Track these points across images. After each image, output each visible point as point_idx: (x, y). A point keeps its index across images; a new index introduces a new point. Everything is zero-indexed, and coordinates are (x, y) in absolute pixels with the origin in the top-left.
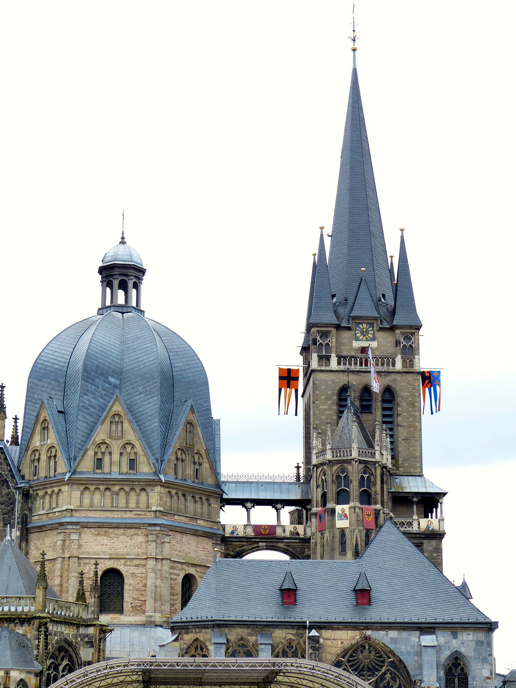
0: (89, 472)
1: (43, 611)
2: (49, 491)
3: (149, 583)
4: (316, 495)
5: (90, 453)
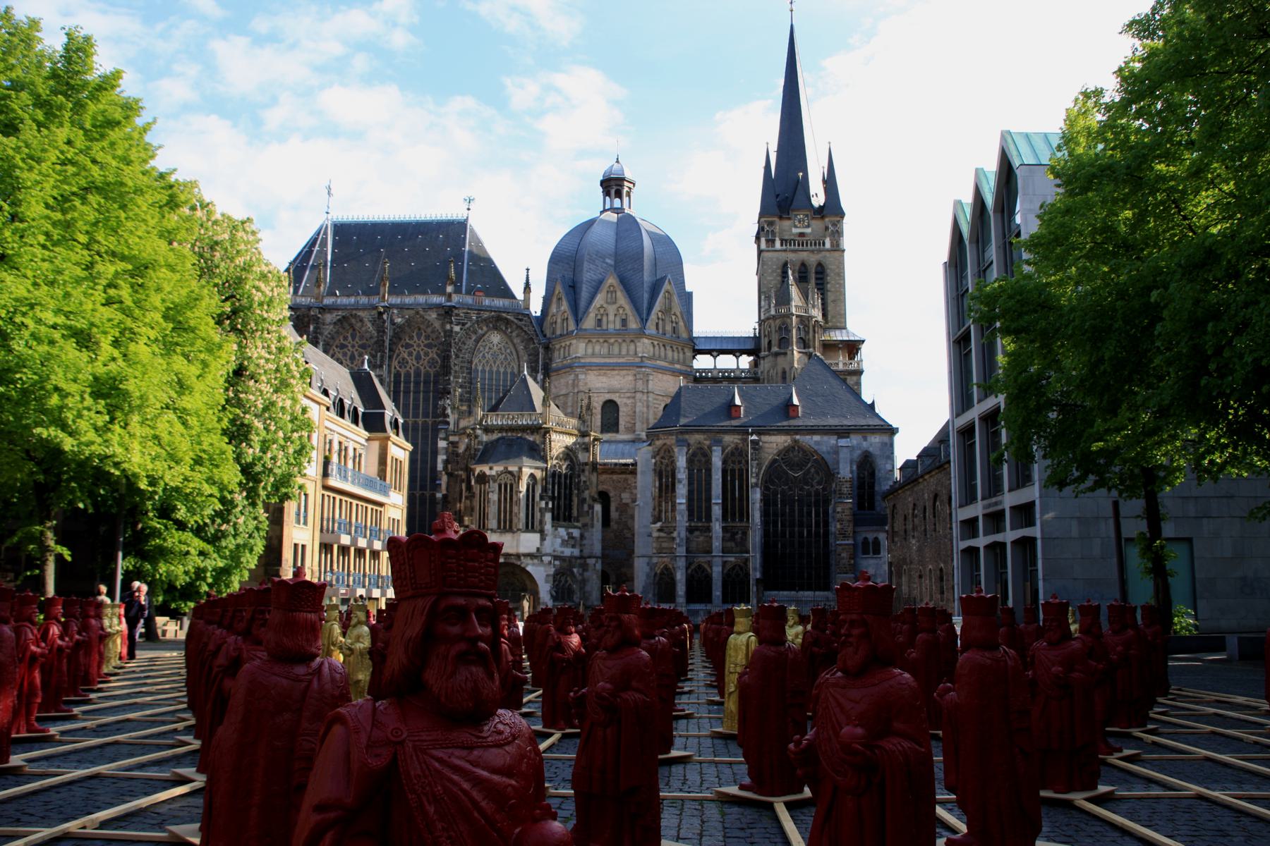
2: (563, 344)
3: (637, 410)
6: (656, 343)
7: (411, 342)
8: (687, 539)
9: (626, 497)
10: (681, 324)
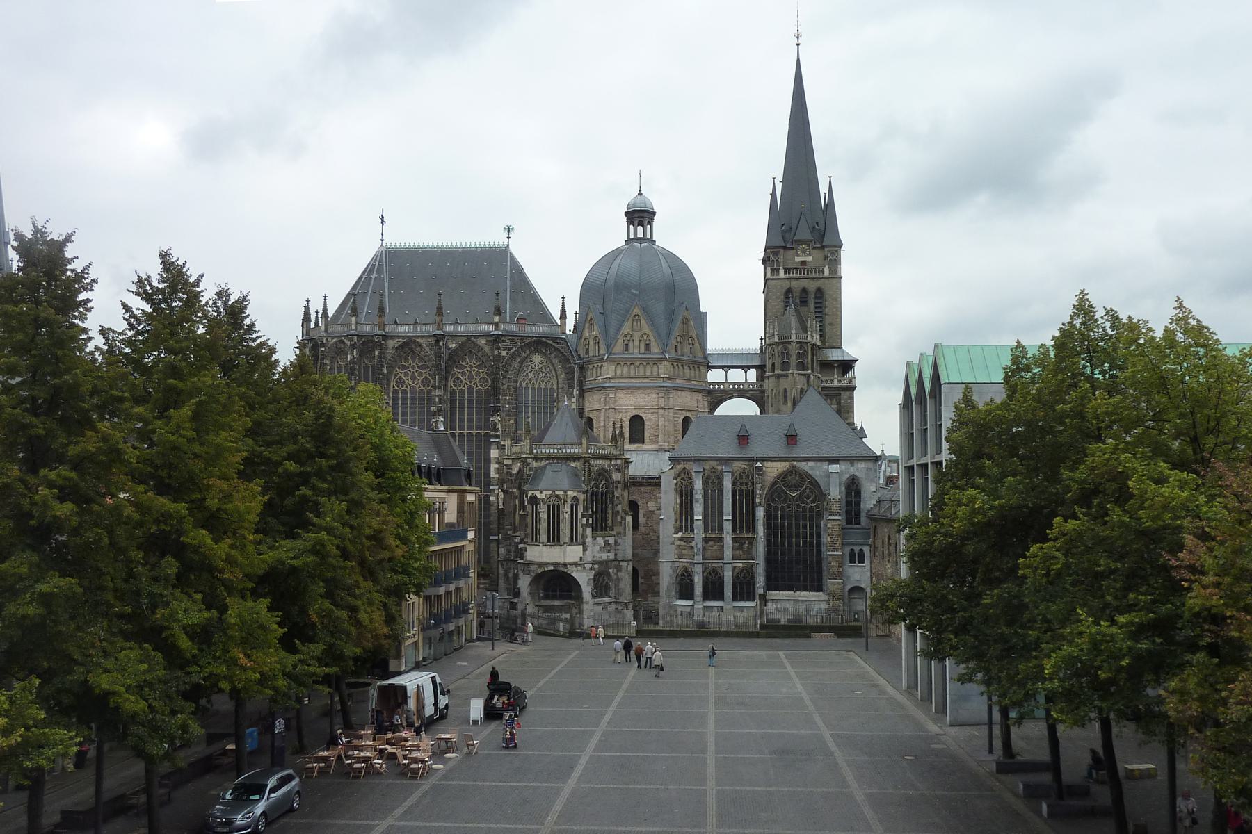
0: (619, 354)
1: (587, 453)
2: (596, 365)
3: (660, 424)
4: (769, 364)
5: (621, 341)
6: (675, 364)
8: (704, 549)
10: (697, 345)
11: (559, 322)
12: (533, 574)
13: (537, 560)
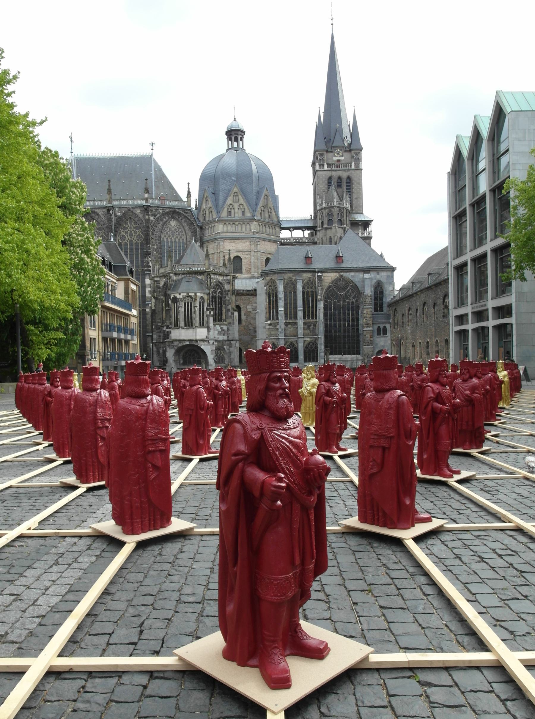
3: (252, 261)
4: (319, 222)
5: (226, 209)
6: (260, 224)
7: (126, 226)
8: (285, 329)
9: (249, 308)
10: (273, 213)
11: (185, 199)
12: (176, 348)
13: (178, 338)
